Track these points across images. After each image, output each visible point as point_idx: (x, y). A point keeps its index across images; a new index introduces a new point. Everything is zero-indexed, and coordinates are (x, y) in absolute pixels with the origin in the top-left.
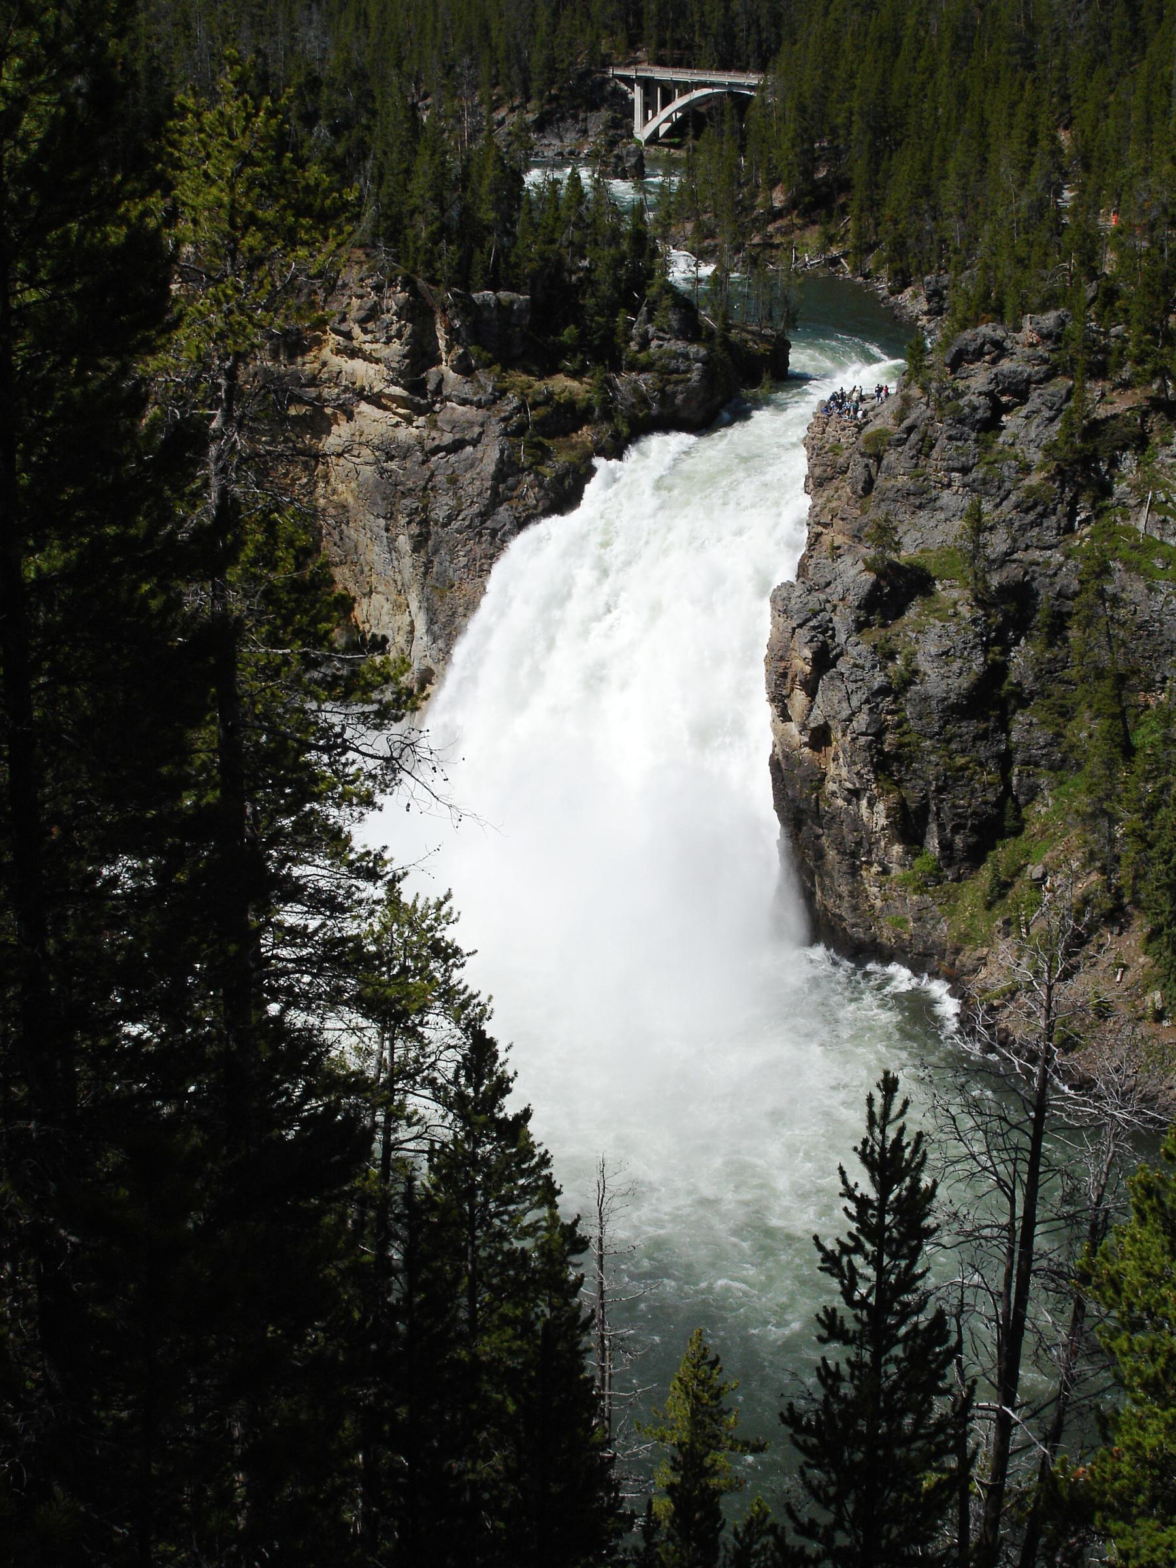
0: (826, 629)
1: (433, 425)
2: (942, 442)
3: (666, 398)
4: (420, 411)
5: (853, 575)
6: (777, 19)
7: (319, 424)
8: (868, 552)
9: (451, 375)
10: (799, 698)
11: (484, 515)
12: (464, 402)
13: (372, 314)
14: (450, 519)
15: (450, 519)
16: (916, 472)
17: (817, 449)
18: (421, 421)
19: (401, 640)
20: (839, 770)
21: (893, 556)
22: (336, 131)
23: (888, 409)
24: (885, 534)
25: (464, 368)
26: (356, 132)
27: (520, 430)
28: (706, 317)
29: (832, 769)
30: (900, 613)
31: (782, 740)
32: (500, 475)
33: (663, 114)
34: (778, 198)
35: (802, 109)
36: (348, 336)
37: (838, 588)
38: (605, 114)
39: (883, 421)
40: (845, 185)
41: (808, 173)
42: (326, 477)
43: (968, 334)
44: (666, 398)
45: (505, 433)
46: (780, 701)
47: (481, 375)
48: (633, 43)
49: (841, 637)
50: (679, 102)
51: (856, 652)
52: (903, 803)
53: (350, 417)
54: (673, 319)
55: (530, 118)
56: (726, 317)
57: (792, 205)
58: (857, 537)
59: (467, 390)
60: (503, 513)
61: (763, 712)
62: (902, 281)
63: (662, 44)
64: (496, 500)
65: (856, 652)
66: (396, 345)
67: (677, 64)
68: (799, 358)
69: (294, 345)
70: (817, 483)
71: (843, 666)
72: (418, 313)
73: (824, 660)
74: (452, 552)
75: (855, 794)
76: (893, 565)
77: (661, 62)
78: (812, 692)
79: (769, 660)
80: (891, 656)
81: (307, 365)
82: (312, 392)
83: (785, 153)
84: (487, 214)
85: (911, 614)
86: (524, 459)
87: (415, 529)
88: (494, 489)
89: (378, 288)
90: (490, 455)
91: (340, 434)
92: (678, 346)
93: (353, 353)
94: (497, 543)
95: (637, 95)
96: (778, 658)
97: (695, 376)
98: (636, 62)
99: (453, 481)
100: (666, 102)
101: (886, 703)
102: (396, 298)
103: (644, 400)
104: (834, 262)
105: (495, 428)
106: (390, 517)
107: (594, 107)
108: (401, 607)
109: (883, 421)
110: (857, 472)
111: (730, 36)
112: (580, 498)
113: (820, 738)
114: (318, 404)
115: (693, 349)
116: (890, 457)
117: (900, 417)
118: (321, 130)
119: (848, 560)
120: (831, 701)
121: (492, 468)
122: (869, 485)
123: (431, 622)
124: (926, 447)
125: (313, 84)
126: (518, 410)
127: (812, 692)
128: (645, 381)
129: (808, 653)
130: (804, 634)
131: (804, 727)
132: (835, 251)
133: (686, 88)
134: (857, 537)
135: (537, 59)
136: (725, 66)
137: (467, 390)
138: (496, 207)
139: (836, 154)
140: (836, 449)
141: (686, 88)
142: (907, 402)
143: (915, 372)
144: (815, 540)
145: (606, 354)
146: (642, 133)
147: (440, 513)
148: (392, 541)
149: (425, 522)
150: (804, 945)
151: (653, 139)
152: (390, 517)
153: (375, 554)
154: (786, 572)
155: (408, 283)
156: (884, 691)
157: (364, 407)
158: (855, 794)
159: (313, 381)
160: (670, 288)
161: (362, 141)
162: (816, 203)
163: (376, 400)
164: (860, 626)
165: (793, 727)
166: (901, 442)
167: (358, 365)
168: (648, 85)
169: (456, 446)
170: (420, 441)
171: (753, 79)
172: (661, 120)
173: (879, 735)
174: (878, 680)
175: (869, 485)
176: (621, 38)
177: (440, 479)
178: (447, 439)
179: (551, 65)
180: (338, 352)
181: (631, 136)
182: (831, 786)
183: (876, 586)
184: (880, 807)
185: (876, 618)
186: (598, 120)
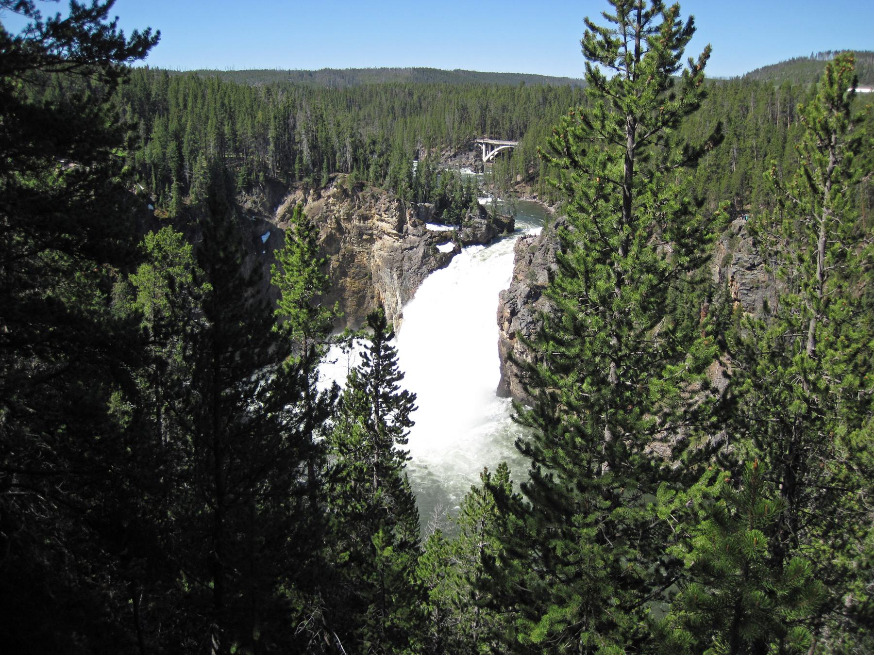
0: (515, 304)
1: (405, 242)
2: (551, 249)
3: (474, 235)
4: (401, 237)
5: (524, 288)
6: (525, 127)
7: (371, 241)
8: (528, 281)
9: (411, 227)
10: (506, 324)
11: (419, 269)
12: (414, 235)
13: (388, 209)
14: (409, 270)
15: (409, 270)
16: (544, 258)
17: (517, 251)
18: (401, 240)
19: (394, 305)
20: (518, 346)
21: (535, 283)
22: (379, 156)
23: (537, 240)
24: (533, 276)
25: (414, 225)
26: (385, 156)
27: (430, 244)
28: (490, 212)
29: (516, 346)
30: (537, 299)
31: (501, 337)
32: (424, 257)
33: (491, 153)
34: (519, 178)
35: (525, 152)
36: (381, 215)
37: (519, 292)
38: (474, 153)
39: (536, 243)
40: (538, 175)
41: (527, 171)
42: (373, 257)
43: (560, 218)
44: (474, 235)
45: (426, 245)
46: (501, 324)
47: (419, 227)
48: (483, 133)
49: (519, 306)
50: (496, 150)
51: (523, 311)
52: (536, 357)
53: (381, 238)
54: (478, 212)
55: (452, 154)
56: (495, 211)
57: (523, 180)
58: (526, 277)
59: (415, 232)
60: (424, 268)
61: (498, 328)
62: (552, 203)
63: (491, 133)
64: (423, 264)
65: (523, 311)
66: (394, 218)
67: (496, 138)
68: (517, 225)
69: (365, 218)
70: (517, 261)
71: (519, 315)
72: (401, 209)
73: (514, 313)
74: (409, 279)
75: (522, 353)
76: (535, 286)
77: (491, 138)
78: (510, 323)
79: (498, 313)
80: (534, 312)
81: (369, 223)
82: (370, 232)
83: (520, 165)
84: (423, 181)
85: (540, 300)
86: (431, 253)
87: (398, 272)
88: (422, 261)
89: (390, 202)
90: (421, 251)
91: (378, 244)
92: (479, 220)
93: (382, 221)
94: (423, 277)
95: (484, 147)
96: (500, 312)
97: (484, 228)
98: (483, 138)
99: (410, 259)
100: (492, 149)
101: (532, 326)
102: (395, 204)
103: (468, 236)
104: (534, 197)
105: (423, 243)
106: (391, 269)
107: (471, 150)
108: (394, 295)
109: (536, 243)
110: (527, 258)
111: (512, 131)
112: (448, 264)
113: (512, 336)
114: (372, 235)
115: (483, 221)
116: (537, 253)
117: (541, 242)
118: (375, 156)
119: (522, 283)
120: (515, 326)
121: (421, 254)
122: (531, 261)
123: (402, 300)
124: (547, 251)
125: (374, 143)
126: (431, 237)
127: (510, 323)
128: (468, 230)
129: (509, 311)
130: (508, 305)
131: (507, 333)
132: (535, 194)
133: (498, 146)
134: (526, 277)
135: (455, 136)
136: (510, 139)
137: (415, 232)
138: (427, 177)
139: (535, 166)
140: (522, 251)
141: (498, 146)
142: (542, 237)
143: (544, 229)
144: (515, 278)
145: (458, 221)
146: (485, 159)
147: (406, 268)
148: (392, 276)
149: (402, 270)
150: (502, 397)
151: (488, 161)
152: (391, 269)
153: (387, 280)
154: (507, 287)
155: (399, 200)
156: (531, 323)
157: (385, 236)
158: (522, 353)
159: (371, 229)
160: (478, 204)
161: (387, 160)
162: (530, 179)
163: (388, 234)
164: (525, 303)
165: (504, 333)
166: (540, 249)
167: (384, 224)
168: (487, 145)
169: (411, 248)
170: (401, 246)
171: (517, 143)
172: (490, 155)
173: (529, 336)
174: (530, 319)
175: (531, 261)
176: (480, 130)
177: (406, 258)
178: (409, 246)
179: (458, 138)
180: (378, 220)
181: (481, 160)
182: (515, 351)
183: (530, 292)
184: (529, 357)
185: (530, 301)
186: (471, 155)
